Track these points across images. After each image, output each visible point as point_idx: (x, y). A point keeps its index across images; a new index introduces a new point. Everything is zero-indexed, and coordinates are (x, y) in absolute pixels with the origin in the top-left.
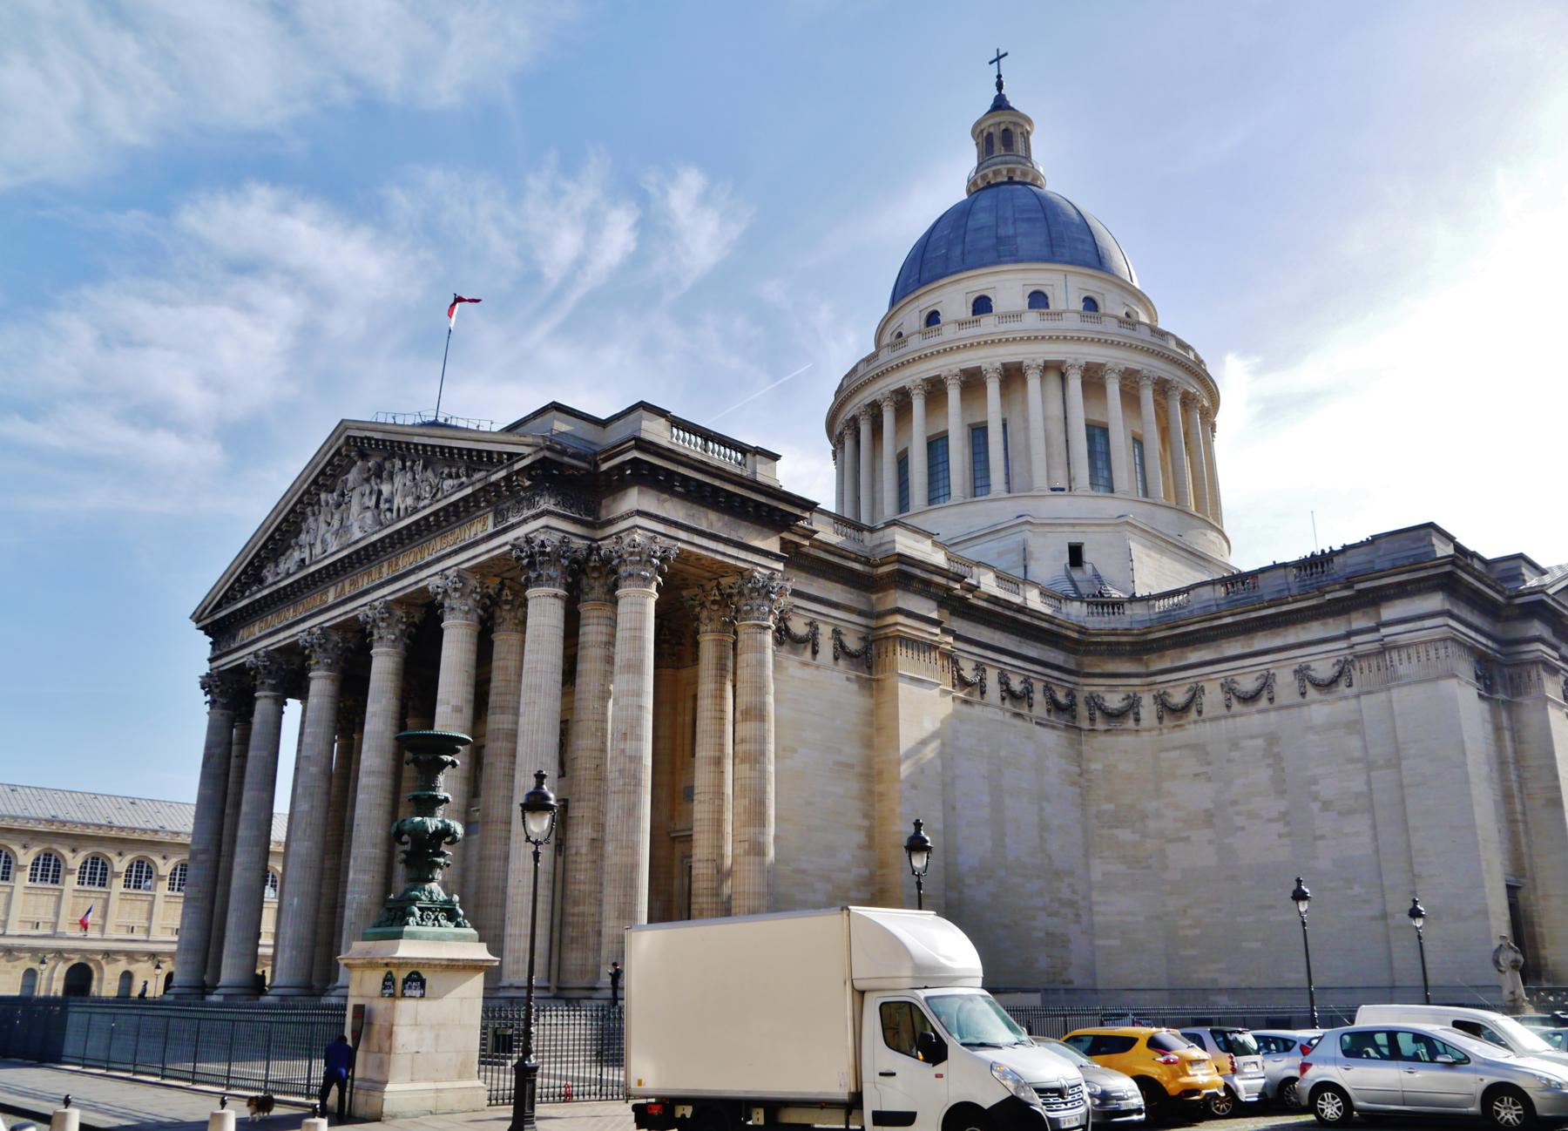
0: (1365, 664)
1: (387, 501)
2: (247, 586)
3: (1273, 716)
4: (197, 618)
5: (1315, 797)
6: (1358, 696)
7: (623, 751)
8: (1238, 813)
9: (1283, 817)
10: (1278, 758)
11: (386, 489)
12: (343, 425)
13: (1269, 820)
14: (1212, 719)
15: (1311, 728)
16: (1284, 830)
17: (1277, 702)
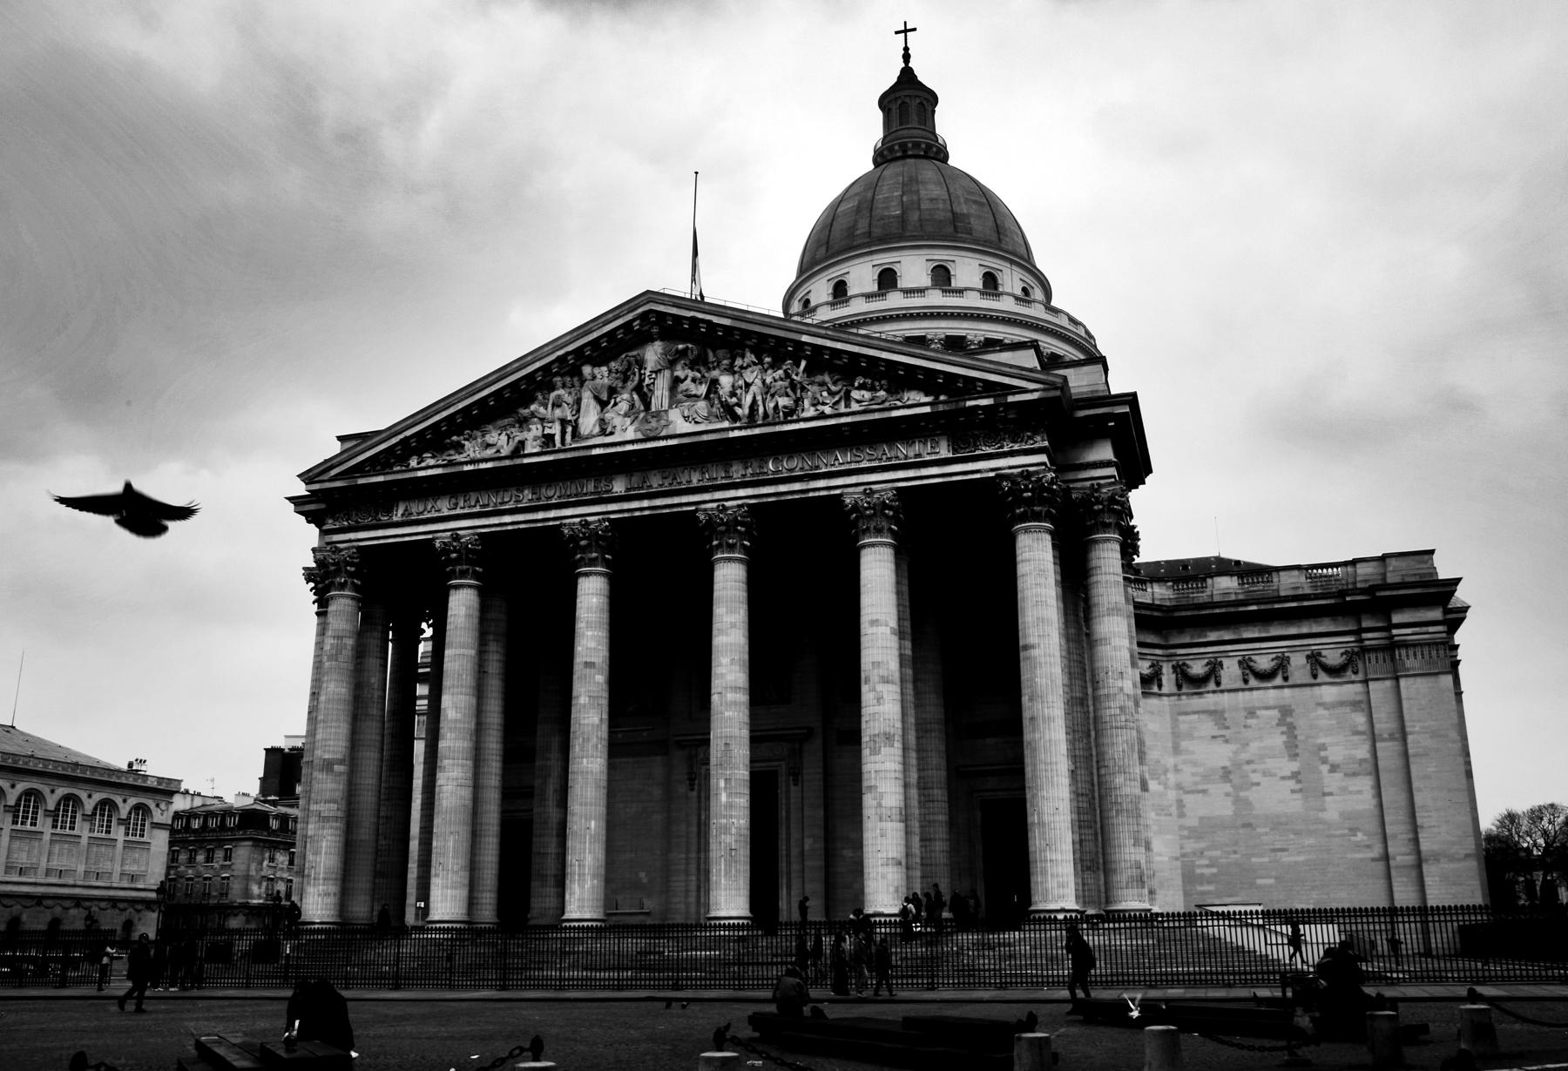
0: (1373, 656)
1: (733, 394)
3: (1286, 691)
4: (307, 477)
5: (1324, 761)
6: (1366, 682)
7: (1121, 689)
8: (1254, 771)
9: (1295, 776)
10: (1291, 728)
11: (726, 381)
12: (649, 296)
13: (1283, 778)
14: (1230, 691)
15: (1319, 704)
16: (1298, 786)
17: (1290, 682)
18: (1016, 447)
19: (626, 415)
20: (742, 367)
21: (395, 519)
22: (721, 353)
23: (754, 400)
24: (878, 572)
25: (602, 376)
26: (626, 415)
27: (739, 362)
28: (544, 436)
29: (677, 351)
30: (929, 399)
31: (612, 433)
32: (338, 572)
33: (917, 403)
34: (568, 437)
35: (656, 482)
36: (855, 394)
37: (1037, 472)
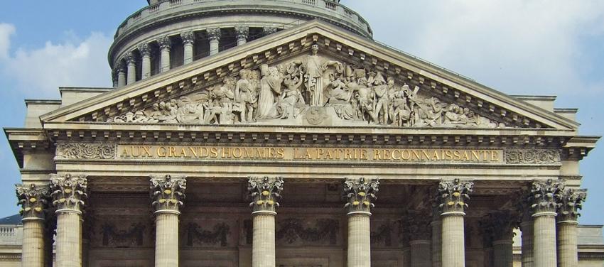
2: (131, 109)
11: (365, 93)
18: (543, 163)
19: (296, 106)
20: (373, 84)
21: (116, 159)
22: (361, 72)
23: (382, 107)
24: (454, 231)
25: (274, 74)
26: (296, 106)
27: (371, 80)
28: (233, 112)
29: (330, 66)
30: (493, 125)
31: (285, 118)
32: (67, 195)
33: (484, 126)
34: (250, 115)
35: (314, 154)
36: (449, 115)
37: (555, 181)
